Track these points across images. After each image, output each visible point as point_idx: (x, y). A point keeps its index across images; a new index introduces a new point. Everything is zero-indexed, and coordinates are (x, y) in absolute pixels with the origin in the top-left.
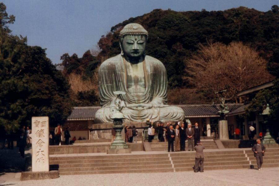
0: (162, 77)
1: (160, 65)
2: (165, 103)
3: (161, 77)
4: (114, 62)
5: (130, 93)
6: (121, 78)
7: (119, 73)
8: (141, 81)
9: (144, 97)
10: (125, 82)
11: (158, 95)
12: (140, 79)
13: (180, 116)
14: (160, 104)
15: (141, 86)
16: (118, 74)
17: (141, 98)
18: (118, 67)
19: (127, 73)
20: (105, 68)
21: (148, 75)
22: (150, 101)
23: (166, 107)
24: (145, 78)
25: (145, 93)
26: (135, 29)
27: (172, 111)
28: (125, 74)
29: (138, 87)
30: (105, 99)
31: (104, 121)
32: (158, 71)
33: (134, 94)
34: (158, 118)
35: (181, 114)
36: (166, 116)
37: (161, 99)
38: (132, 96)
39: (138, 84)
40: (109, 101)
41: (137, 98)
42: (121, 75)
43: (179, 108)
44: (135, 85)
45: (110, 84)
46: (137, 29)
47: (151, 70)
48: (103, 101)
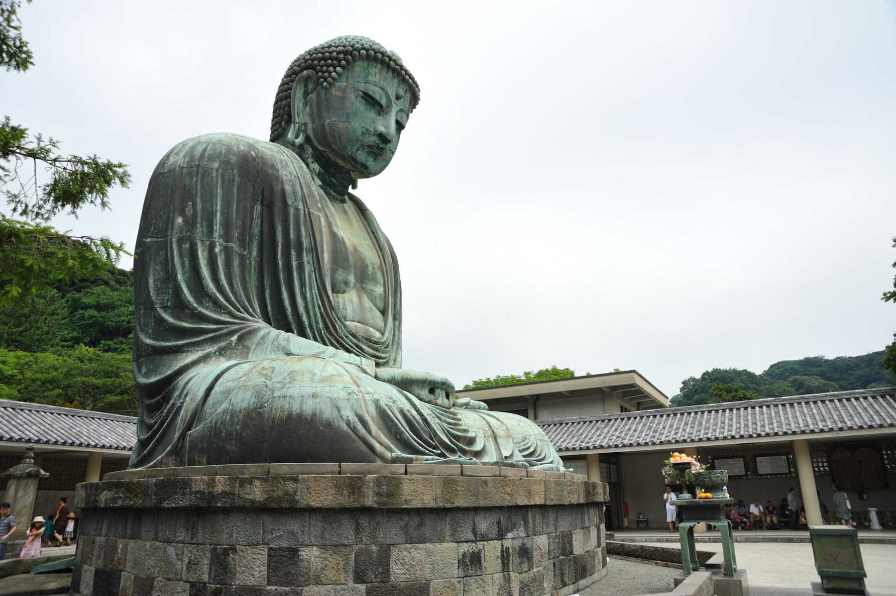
5: (345, 318)
7: (301, 207)
8: (375, 280)
12: (370, 269)
15: (373, 300)
16: (292, 210)
20: (233, 159)
39: (364, 289)
40: (232, 333)
41: (370, 347)
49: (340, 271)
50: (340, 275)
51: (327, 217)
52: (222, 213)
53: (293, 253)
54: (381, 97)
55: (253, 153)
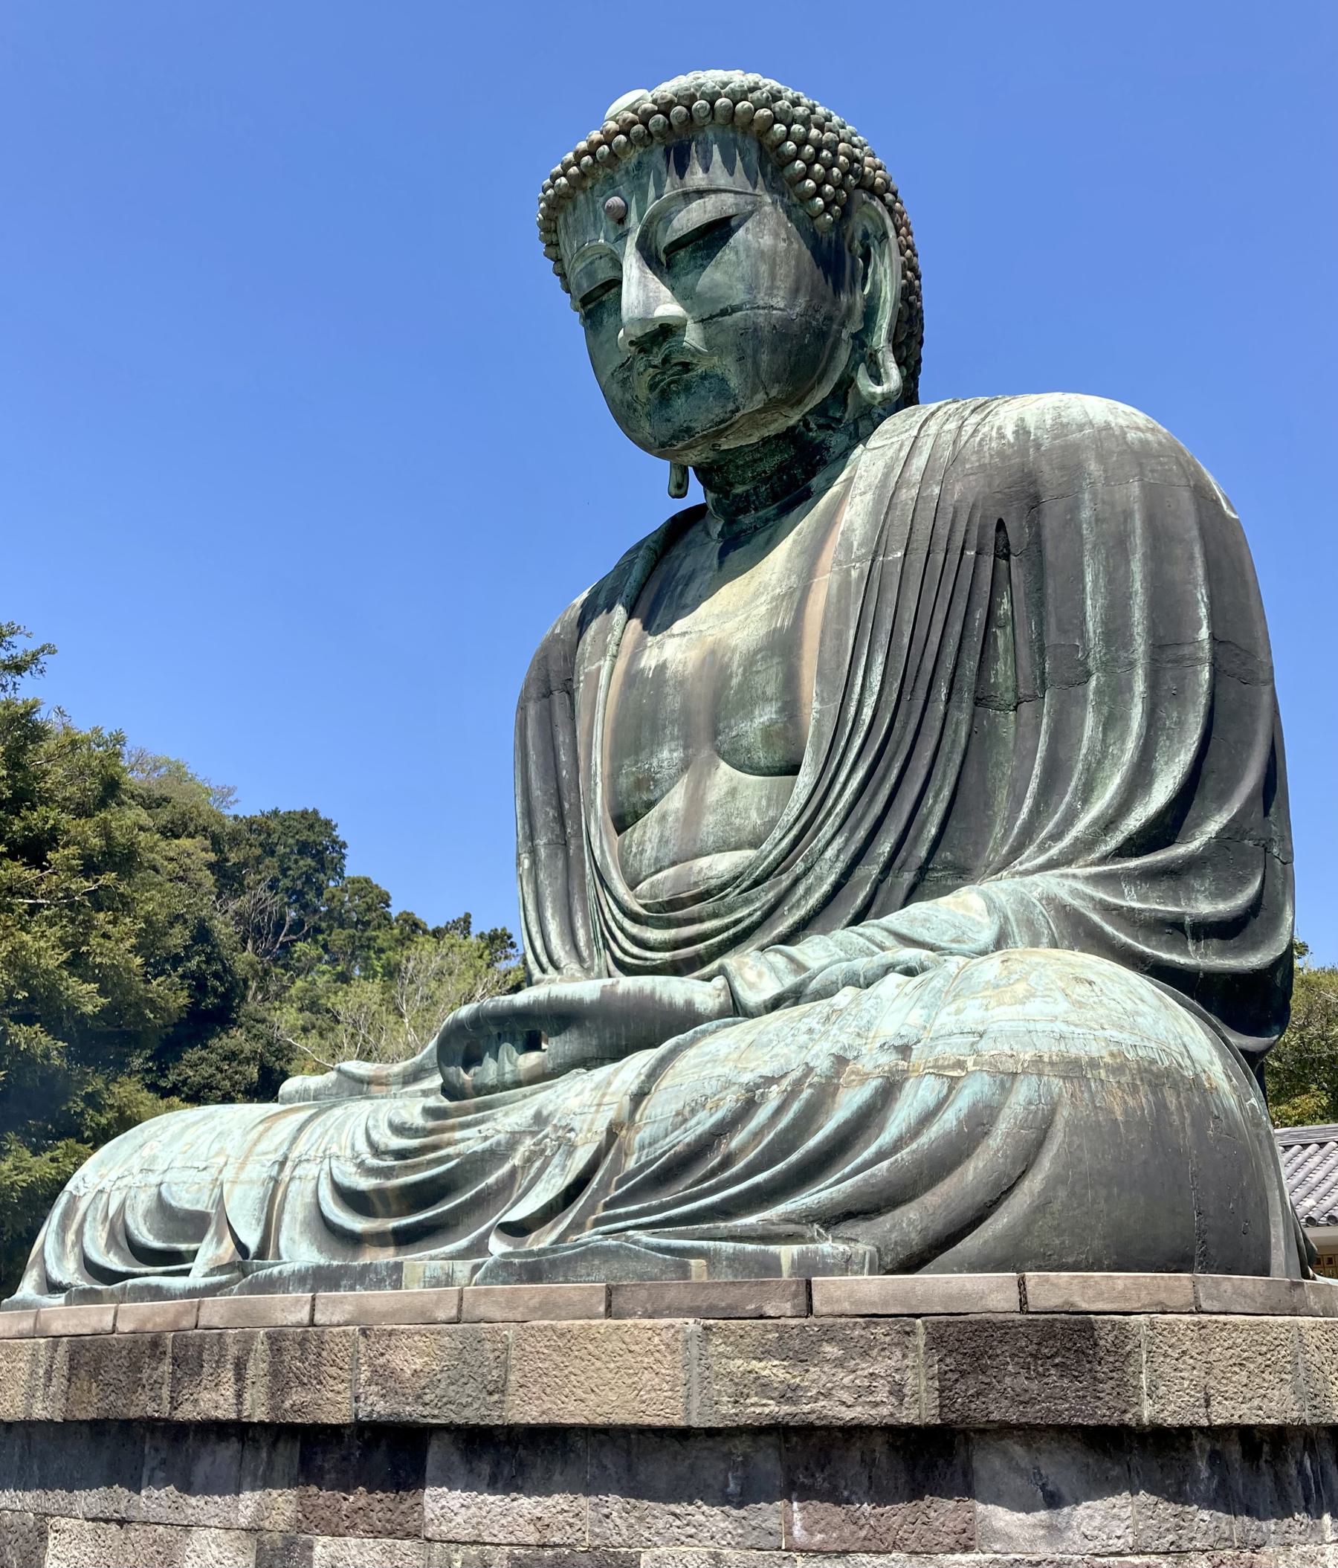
0: (1089, 578)
1: (1055, 438)
9: (766, 895)
12: (735, 682)
37: (1070, 885)
38: (635, 918)
41: (670, 924)
44: (685, 765)
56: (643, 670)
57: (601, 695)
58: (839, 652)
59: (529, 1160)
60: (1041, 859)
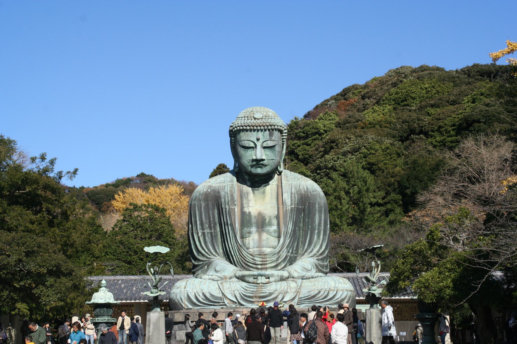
0: (317, 216)
2: (319, 269)
3: (315, 215)
4: (218, 185)
5: (248, 249)
6: (230, 218)
8: (270, 224)
9: (276, 256)
10: (237, 226)
11: (306, 254)
12: (267, 220)
13: (343, 297)
14: (308, 270)
16: (224, 210)
17: (268, 259)
18: (225, 196)
19: (242, 207)
21: (286, 210)
22: (288, 265)
23: (317, 277)
24: (278, 217)
25: (278, 249)
26: (258, 119)
27: (326, 287)
28: (237, 209)
29: (265, 236)
30: (199, 260)
31: (184, 305)
32: (309, 203)
33: (255, 249)
34: (296, 300)
35: (345, 293)
36: (314, 296)
37: (314, 260)
40: (205, 265)
41: (260, 258)
42: (229, 212)
43: (342, 280)
44: (257, 231)
45: (209, 231)
46: (262, 119)
47: (293, 202)
48: (196, 263)
49: (245, 229)
50: (246, 230)
51: (242, 205)
52: (199, 220)
53: (226, 227)
54: (249, 144)
55: (209, 190)
56: (245, 212)
57: (236, 214)
58: (287, 221)
59: (279, 294)
60: (310, 256)
